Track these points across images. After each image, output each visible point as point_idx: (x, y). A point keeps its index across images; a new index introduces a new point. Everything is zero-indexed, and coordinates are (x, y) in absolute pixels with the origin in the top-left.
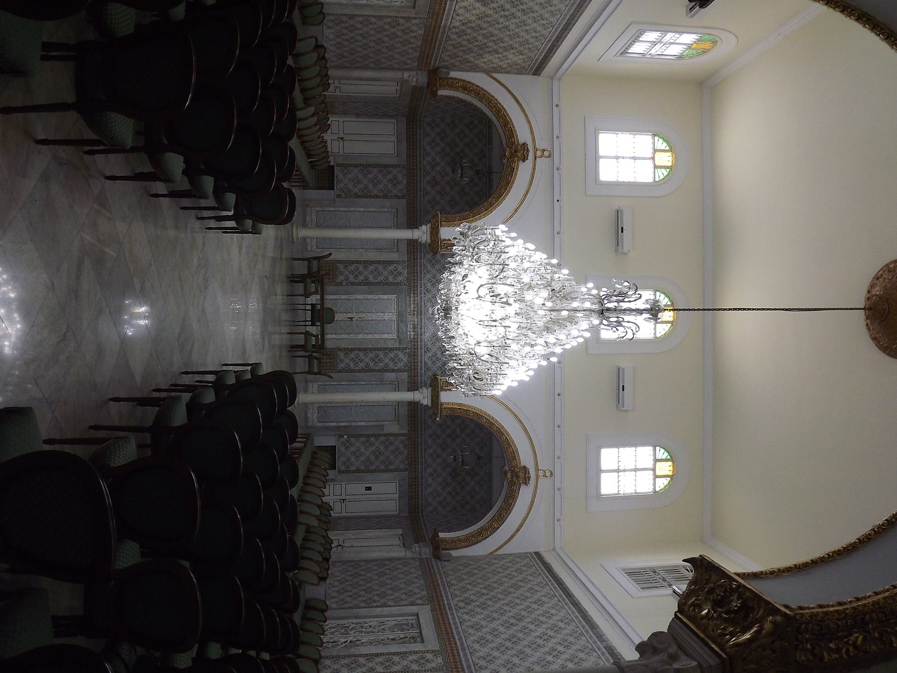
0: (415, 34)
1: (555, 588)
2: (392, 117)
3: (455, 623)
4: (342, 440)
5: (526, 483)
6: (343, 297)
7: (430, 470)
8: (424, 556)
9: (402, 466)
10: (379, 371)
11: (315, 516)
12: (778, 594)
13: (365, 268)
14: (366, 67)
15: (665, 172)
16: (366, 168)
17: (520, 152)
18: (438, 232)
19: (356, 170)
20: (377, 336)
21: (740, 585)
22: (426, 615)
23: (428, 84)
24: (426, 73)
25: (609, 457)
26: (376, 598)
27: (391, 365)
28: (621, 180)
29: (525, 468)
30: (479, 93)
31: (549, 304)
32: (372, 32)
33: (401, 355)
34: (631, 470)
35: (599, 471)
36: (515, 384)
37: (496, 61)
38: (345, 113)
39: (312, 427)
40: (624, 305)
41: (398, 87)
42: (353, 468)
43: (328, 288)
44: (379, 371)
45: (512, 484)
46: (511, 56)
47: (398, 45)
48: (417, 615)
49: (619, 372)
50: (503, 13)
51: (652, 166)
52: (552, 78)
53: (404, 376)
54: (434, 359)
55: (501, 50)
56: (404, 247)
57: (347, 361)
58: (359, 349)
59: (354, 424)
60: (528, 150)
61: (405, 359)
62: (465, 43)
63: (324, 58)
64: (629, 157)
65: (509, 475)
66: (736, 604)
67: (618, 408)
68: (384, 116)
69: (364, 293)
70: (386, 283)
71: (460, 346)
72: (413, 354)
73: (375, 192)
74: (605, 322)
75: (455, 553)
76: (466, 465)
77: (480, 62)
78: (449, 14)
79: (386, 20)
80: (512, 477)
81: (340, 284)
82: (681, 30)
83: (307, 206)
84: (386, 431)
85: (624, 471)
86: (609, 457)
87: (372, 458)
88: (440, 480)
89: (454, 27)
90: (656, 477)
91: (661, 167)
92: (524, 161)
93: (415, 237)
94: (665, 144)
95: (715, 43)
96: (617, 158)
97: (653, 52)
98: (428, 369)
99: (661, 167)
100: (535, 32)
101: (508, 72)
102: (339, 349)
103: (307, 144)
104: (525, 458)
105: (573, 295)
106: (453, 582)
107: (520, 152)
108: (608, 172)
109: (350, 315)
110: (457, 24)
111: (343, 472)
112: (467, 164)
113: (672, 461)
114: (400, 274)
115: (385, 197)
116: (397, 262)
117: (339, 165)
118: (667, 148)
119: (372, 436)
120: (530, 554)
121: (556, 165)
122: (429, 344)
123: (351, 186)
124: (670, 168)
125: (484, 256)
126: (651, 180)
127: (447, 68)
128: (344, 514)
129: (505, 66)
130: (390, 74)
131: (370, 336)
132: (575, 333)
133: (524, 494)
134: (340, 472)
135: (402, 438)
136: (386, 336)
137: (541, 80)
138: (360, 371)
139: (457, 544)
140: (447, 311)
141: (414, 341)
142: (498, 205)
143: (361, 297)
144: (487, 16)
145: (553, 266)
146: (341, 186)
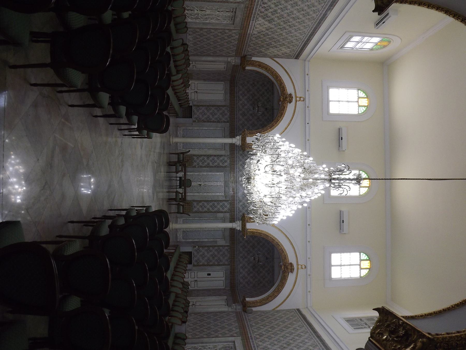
0: (234, 38)
1: (308, 328)
2: (222, 81)
3: (254, 347)
4: (195, 248)
5: (292, 272)
6: (196, 174)
7: (241, 265)
8: (238, 311)
9: (226, 263)
10: (215, 212)
11: (180, 288)
12: (425, 327)
13: (208, 158)
14: (209, 55)
15: (364, 109)
16: (208, 107)
17: (288, 98)
18: (245, 139)
19: (203, 108)
20: (214, 194)
21: (404, 323)
22: (238, 342)
24: (240, 58)
25: (336, 258)
26: (213, 333)
27: (221, 209)
28: (341, 113)
29: (291, 264)
31: (302, 176)
32: (212, 37)
34: (348, 265)
35: (330, 266)
36: (285, 218)
37: (276, 52)
38: (198, 79)
39: (180, 242)
40: (342, 177)
42: (201, 264)
43: (188, 169)
44: (215, 212)
45: (284, 272)
46: (283, 49)
47: (225, 44)
48: (234, 342)
49: (341, 213)
50: (279, 27)
52: (305, 60)
53: (228, 215)
54: (243, 206)
55: (278, 46)
56: (228, 148)
57: (198, 207)
59: (201, 240)
60: (292, 97)
61: (228, 206)
62: (260, 42)
63: (187, 50)
64: (345, 101)
65: (283, 267)
66: (402, 332)
67: (340, 232)
68: (218, 80)
69: (207, 171)
70: (218, 166)
71: (255, 198)
72: (232, 204)
73: (213, 119)
74: (332, 185)
75: (254, 309)
76: (260, 262)
77: (267, 52)
78: (251, 28)
79: (219, 31)
80: (284, 268)
81: (195, 167)
82: (372, 35)
84: (218, 244)
85: (344, 265)
86: (336, 258)
87: (211, 258)
88: (246, 270)
89: (254, 34)
91: (362, 106)
92: (290, 103)
93: (234, 142)
94: (364, 94)
95: (390, 42)
96: (339, 101)
97: (357, 47)
98: (240, 211)
99: (362, 106)
100: (296, 37)
101: (282, 58)
102: (194, 201)
103: (178, 94)
104: (291, 258)
105: (315, 171)
106: (254, 324)
107: (288, 98)
108: (334, 109)
109: (199, 183)
110: (256, 33)
112: (261, 104)
114: (226, 161)
115: (218, 122)
116: (225, 156)
117: (194, 105)
118: (365, 96)
119: (211, 246)
120: (294, 309)
121: (307, 105)
122: (241, 198)
123: (201, 116)
124: (367, 106)
125: (268, 151)
126: (357, 113)
127: (250, 55)
128: (196, 288)
129: (280, 54)
130: (221, 59)
131: (210, 194)
132: (316, 191)
133: (291, 277)
134: (194, 266)
135: (226, 248)
136: (218, 194)
137: (299, 61)
138: (205, 212)
140: (249, 179)
141: (233, 196)
142: (277, 125)
143: (205, 174)
144: (271, 28)
145: (305, 156)
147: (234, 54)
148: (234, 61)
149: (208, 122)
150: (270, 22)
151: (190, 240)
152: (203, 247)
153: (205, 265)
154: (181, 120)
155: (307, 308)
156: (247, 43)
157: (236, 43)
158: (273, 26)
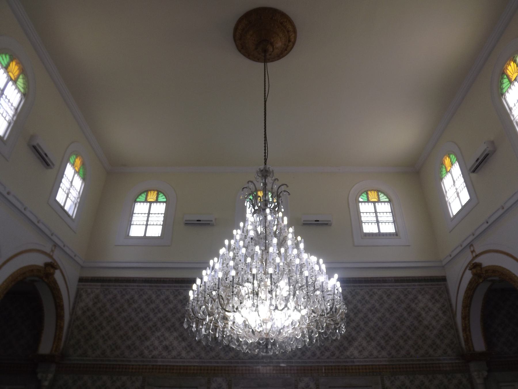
51: (155, 204)
64: (148, 219)
90: (379, 201)
91: (157, 197)
99: (157, 197)
113: (367, 191)
118: (145, 193)
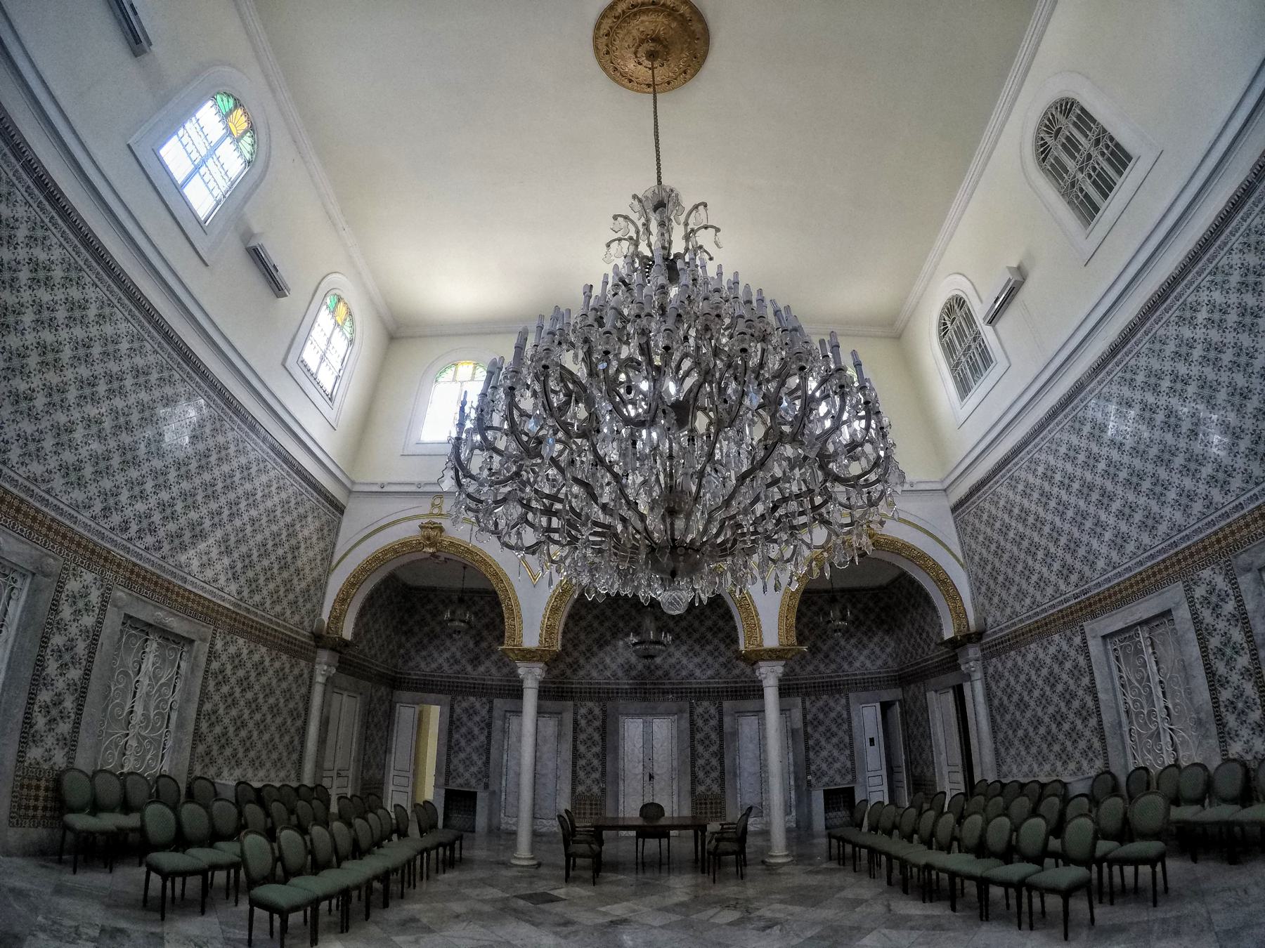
4: (813, 781)
8: (979, 654)
9: (843, 701)
13: (582, 757)
14: (303, 731)
23: (333, 649)
27: (713, 722)
30: (354, 583)
33: (700, 710)
39: (797, 823)
41: (345, 694)
42: (849, 764)
52: (350, 492)
53: (727, 705)
57: (708, 781)
58: (693, 765)
61: (706, 704)
73: (483, 738)
78: (211, 593)
79: (211, 687)
81: (603, 791)
83: (499, 829)
87: (835, 740)
88: (855, 652)
92: (441, 529)
94: (449, 371)
102: (693, 791)
110: (233, 587)
111: (854, 777)
114: (591, 711)
115: (489, 725)
116: (575, 713)
120: (955, 519)
123: (474, 769)
134: (854, 779)
135: (808, 703)
137: (352, 506)
139: (959, 614)
146: (473, 782)
147: (303, 663)
148: (324, 665)
149: (488, 751)
150: (199, 536)
151: (793, 796)
152: (808, 761)
153: (852, 752)
154: (481, 821)
155: (945, 490)
156: (291, 630)
157: (263, 650)
158: (219, 533)
